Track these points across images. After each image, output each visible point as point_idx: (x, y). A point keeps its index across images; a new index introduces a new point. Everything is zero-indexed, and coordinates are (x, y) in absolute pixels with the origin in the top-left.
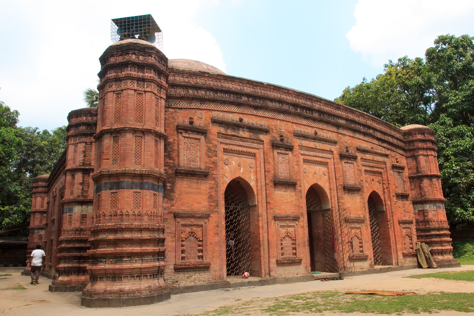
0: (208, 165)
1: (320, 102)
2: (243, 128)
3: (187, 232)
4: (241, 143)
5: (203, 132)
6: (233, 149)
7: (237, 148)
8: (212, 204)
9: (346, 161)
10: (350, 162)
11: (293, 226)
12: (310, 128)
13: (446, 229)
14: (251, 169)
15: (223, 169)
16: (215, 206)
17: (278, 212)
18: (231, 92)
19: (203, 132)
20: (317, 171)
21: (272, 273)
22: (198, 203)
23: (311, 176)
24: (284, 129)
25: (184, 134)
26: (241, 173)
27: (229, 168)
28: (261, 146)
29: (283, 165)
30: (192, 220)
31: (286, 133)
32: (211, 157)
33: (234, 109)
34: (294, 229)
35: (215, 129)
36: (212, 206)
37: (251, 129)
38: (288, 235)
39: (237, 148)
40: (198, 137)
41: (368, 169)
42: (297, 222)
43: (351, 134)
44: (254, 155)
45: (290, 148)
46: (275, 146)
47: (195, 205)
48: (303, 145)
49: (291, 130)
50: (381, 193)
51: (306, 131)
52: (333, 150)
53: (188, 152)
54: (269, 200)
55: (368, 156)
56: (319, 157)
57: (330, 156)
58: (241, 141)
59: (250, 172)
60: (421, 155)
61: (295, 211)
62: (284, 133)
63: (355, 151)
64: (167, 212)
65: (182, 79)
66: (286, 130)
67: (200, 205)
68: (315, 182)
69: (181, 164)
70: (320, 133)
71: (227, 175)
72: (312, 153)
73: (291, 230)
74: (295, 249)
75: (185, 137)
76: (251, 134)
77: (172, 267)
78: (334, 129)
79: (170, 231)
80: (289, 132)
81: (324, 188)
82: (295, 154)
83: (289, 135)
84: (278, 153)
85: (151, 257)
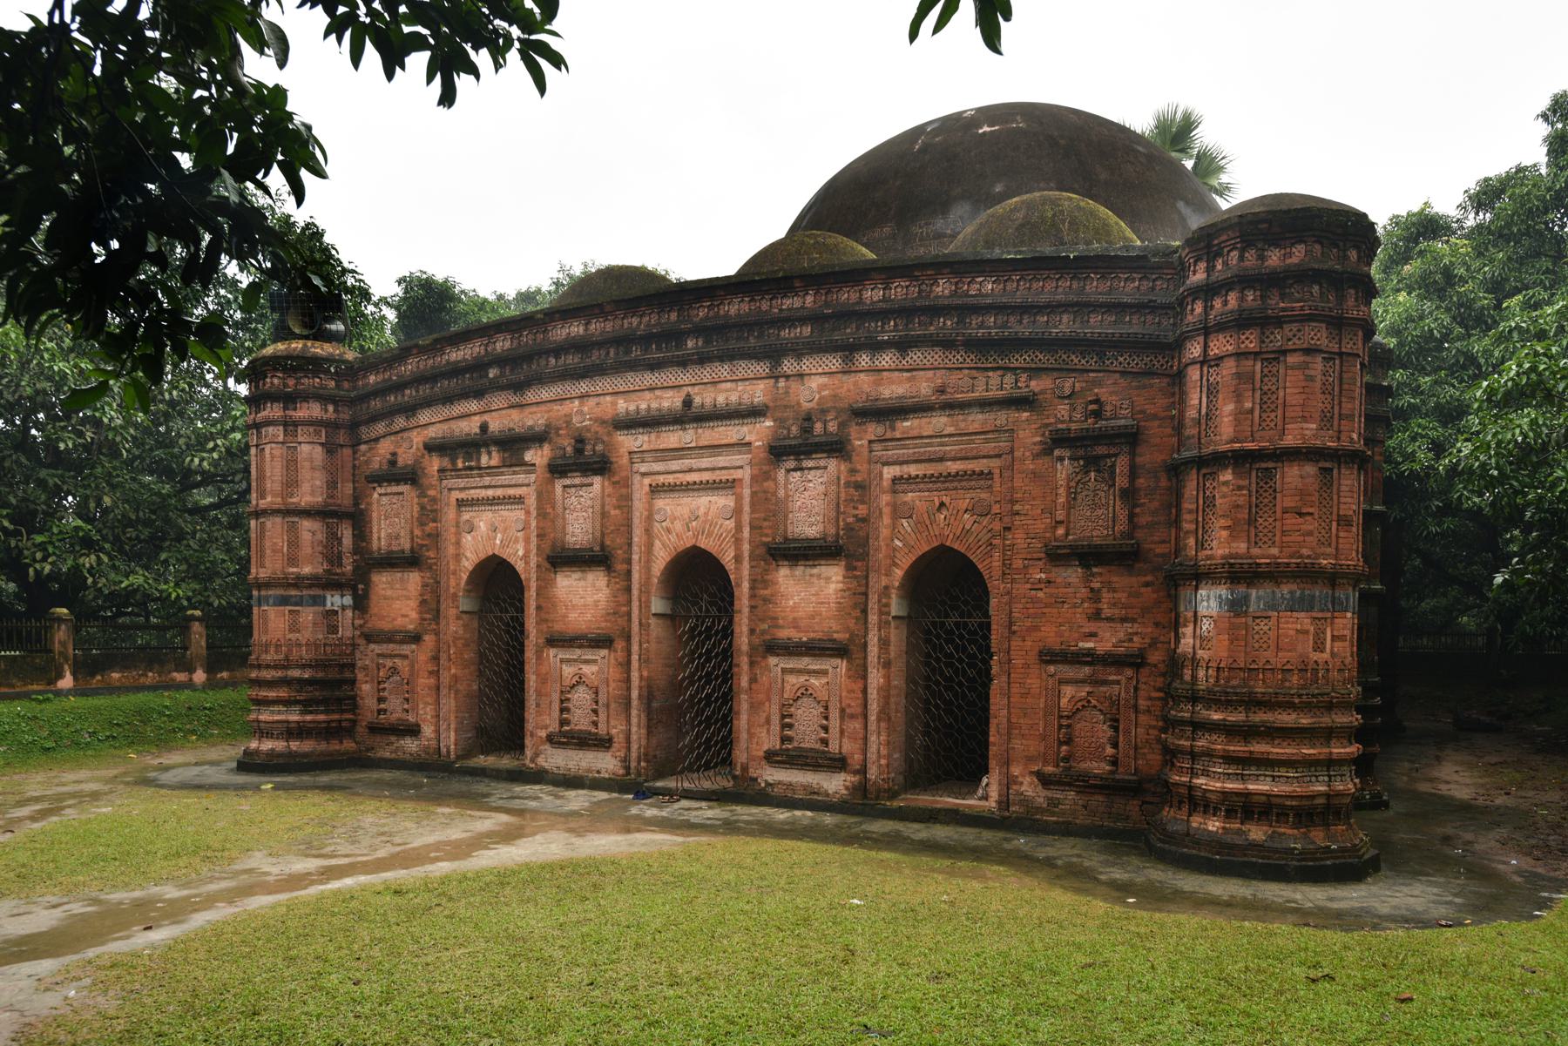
2: (486, 444)
4: (487, 480)
5: (411, 476)
7: (483, 493)
9: (791, 464)
10: (810, 464)
12: (670, 393)
13: (1344, 706)
15: (458, 543)
17: (558, 627)
19: (411, 476)
23: (678, 526)
25: (379, 490)
26: (497, 546)
28: (533, 477)
29: (581, 511)
30: (391, 646)
31: (596, 428)
33: (474, 406)
35: (434, 464)
38: (580, 681)
41: (913, 470)
42: (604, 652)
43: (834, 362)
44: (519, 500)
45: (602, 466)
46: (557, 469)
48: (645, 447)
49: (608, 413)
51: (654, 405)
52: (747, 439)
55: (907, 425)
56: (700, 470)
58: (489, 475)
59: (517, 541)
60: (1194, 363)
63: (842, 425)
64: (357, 633)
66: (596, 420)
70: (705, 398)
72: (675, 465)
73: (587, 670)
74: (595, 712)
78: (762, 368)
80: (604, 422)
81: (719, 557)
82: (616, 478)
83: (601, 430)
85: (281, 708)
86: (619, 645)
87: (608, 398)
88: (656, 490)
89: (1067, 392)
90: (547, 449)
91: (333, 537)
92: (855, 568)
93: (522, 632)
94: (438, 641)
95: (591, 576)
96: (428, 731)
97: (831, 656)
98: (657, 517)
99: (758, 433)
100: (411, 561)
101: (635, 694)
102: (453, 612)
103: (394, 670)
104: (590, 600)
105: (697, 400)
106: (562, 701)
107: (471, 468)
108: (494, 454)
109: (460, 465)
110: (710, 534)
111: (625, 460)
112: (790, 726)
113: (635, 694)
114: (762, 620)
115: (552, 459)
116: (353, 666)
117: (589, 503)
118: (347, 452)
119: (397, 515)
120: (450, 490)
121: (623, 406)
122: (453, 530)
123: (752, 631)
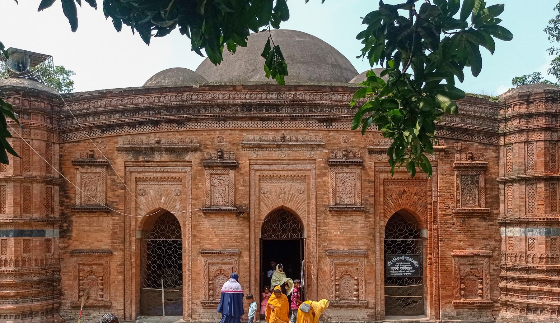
0: (111, 200)
1: (296, 90)
2: (159, 150)
3: (86, 271)
4: (158, 169)
6: (149, 177)
8: (115, 241)
9: (337, 170)
10: (348, 170)
11: (230, 263)
12: (273, 133)
14: (177, 197)
16: (119, 243)
17: (206, 246)
18: (143, 109)
20: (287, 190)
21: (193, 316)
22: (98, 241)
23: (273, 196)
24: (226, 142)
25: (81, 170)
26: (163, 203)
27: (146, 198)
28: (189, 168)
31: (229, 146)
32: (116, 191)
34: (231, 266)
36: (116, 243)
37: (170, 150)
39: (155, 175)
40: (98, 170)
42: (236, 258)
44: (180, 180)
47: (96, 243)
48: (258, 157)
50: (419, 211)
51: (264, 137)
52: (314, 157)
53: (87, 188)
54: (195, 232)
56: (288, 170)
57: (308, 166)
59: (175, 201)
61: (235, 244)
62: (225, 147)
65: (81, 107)
66: (230, 142)
67: (102, 243)
68: (281, 204)
69: (78, 202)
71: (142, 207)
72: (274, 167)
73: (225, 267)
75: (81, 173)
76: (172, 156)
77: (68, 304)
78: (324, 126)
79: (67, 270)
80: (234, 144)
84: (211, 174)
86: (245, 254)
87: (237, 132)
88: (261, 179)
89: (459, 149)
90: (198, 155)
91: (49, 197)
92: (369, 217)
93: (181, 249)
94: (124, 255)
95: (227, 220)
96: (118, 305)
97: (359, 256)
98: (262, 191)
99: (319, 155)
100: (107, 211)
101: (253, 278)
102: (134, 238)
103: (91, 272)
104: (227, 232)
105: (288, 137)
106: (209, 284)
107: (148, 162)
108: (164, 155)
109: (141, 159)
110: (291, 200)
111: (247, 163)
113: (253, 278)
114: (324, 241)
115: (202, 160)
116: (59, 271)
117: (227, 183)
118: (57, 147)
119: (95, 184)
120: (131, 172)
121: (246, 136)
122: (133, 194)
123: (318, 246)
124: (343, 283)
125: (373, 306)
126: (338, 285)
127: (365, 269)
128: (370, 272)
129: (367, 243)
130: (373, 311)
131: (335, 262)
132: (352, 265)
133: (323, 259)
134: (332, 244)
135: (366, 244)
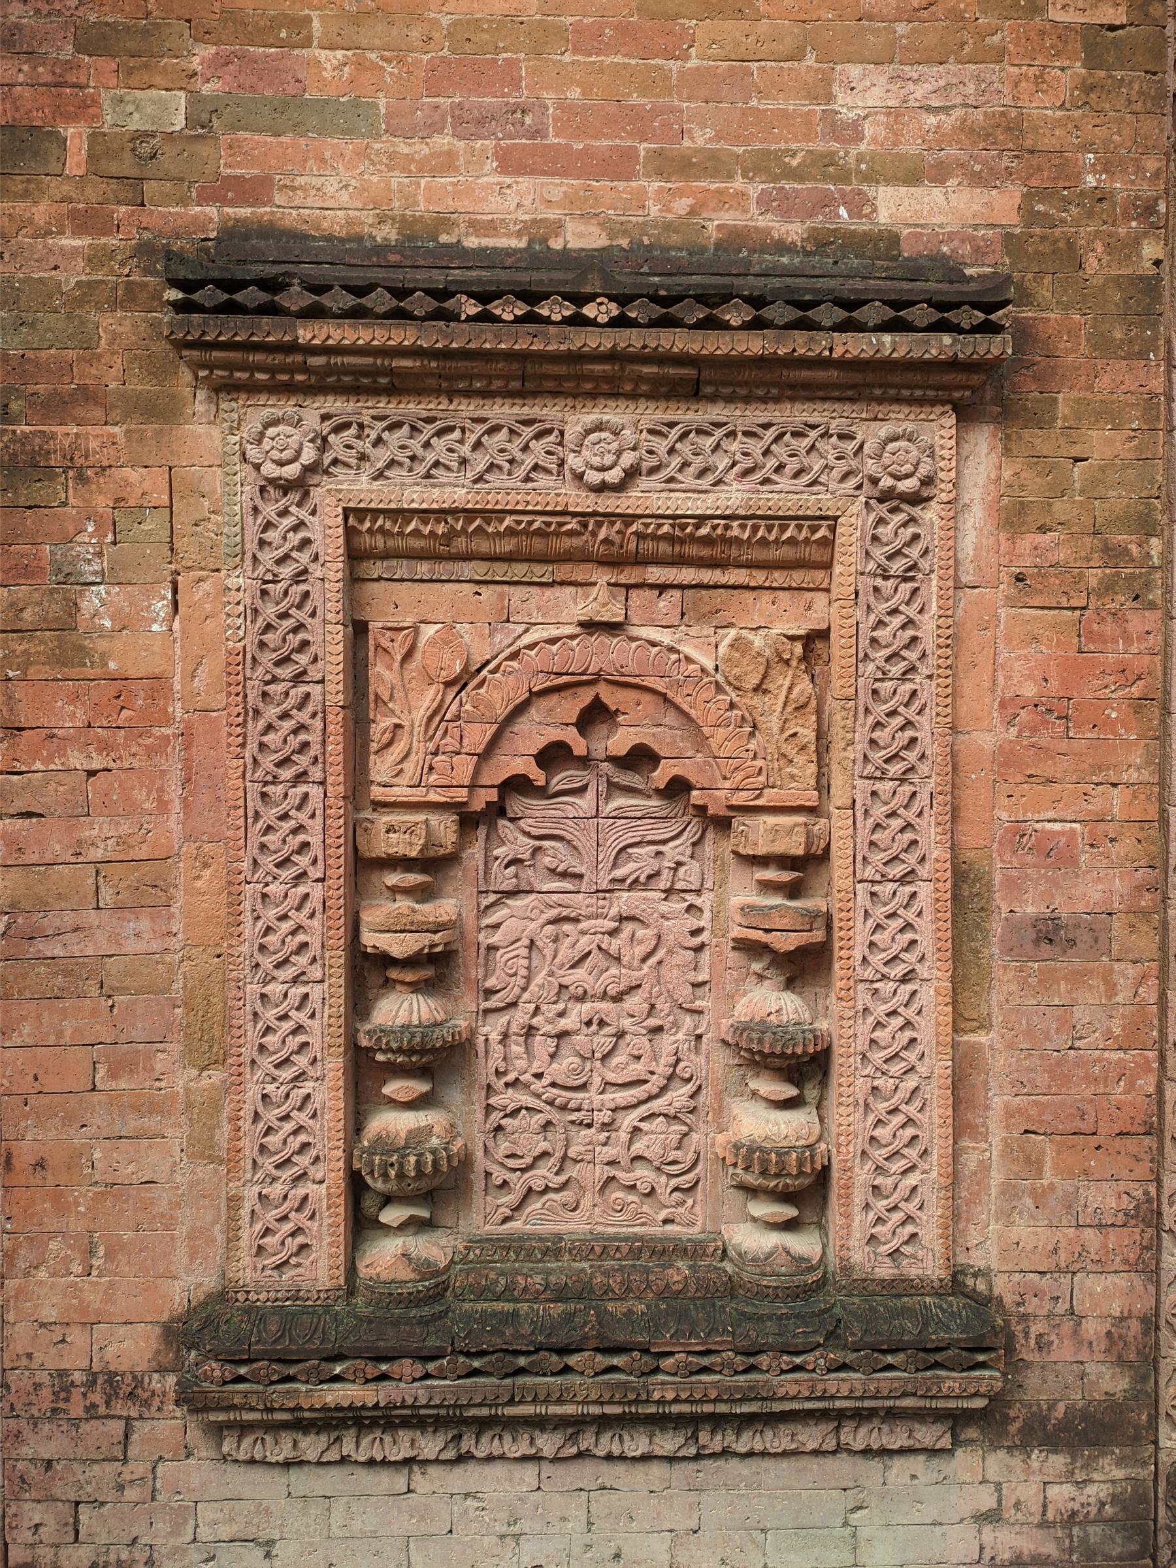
112: (437, 1062)
124: (516, 920)
125: (1112, 1382)
126: (436, 968)
127: (953, 641)
128: (1056, 711)
129: (1009, 130)
130: (1107, 1477)
131: (360, 488)
132: (705, 552)
133: (96, 437)
134: (292, 112)
135: (1003, 141)
